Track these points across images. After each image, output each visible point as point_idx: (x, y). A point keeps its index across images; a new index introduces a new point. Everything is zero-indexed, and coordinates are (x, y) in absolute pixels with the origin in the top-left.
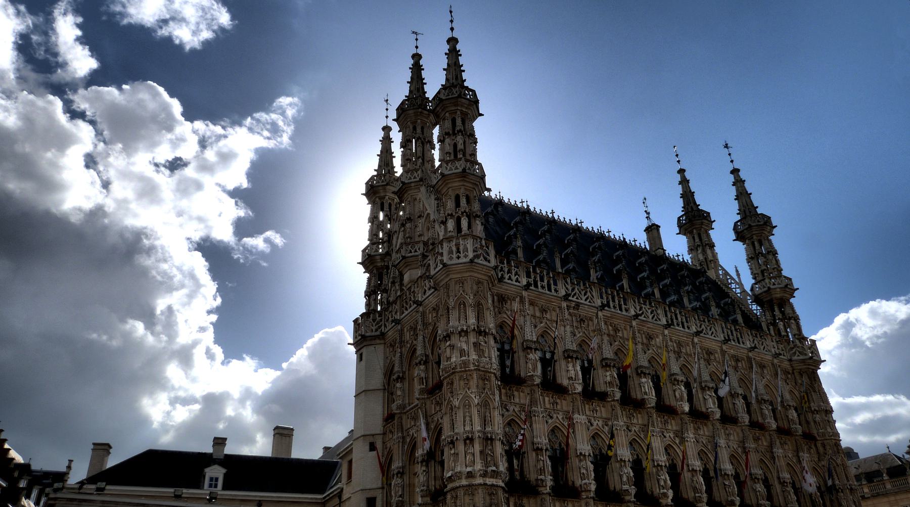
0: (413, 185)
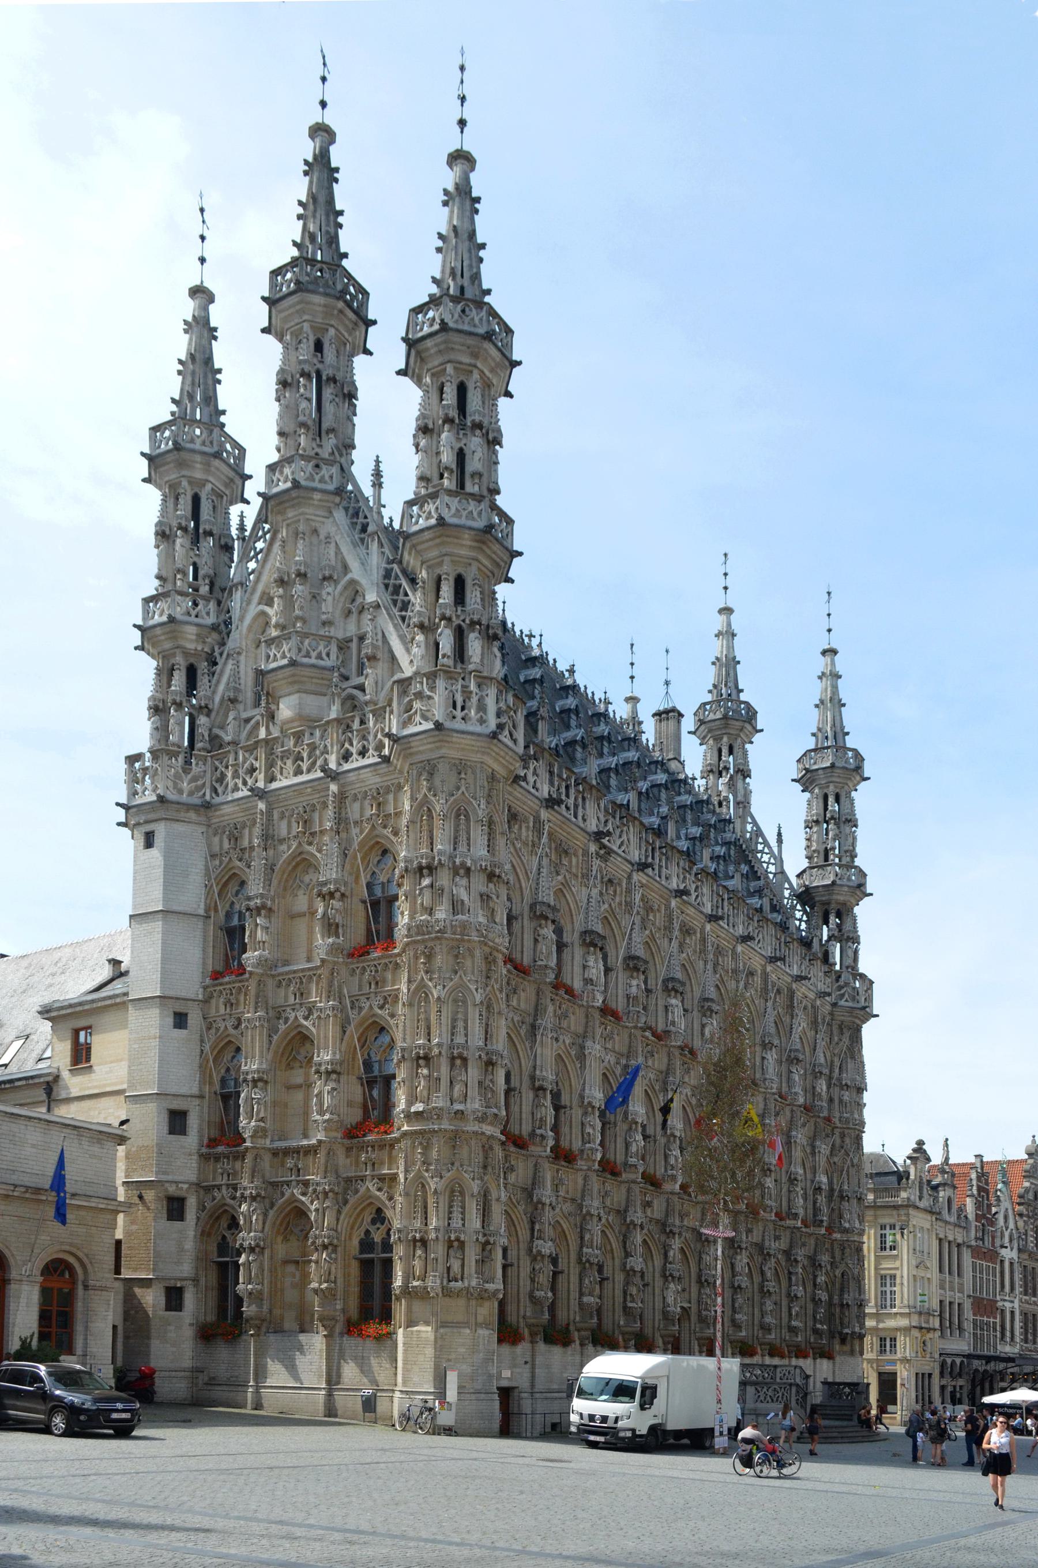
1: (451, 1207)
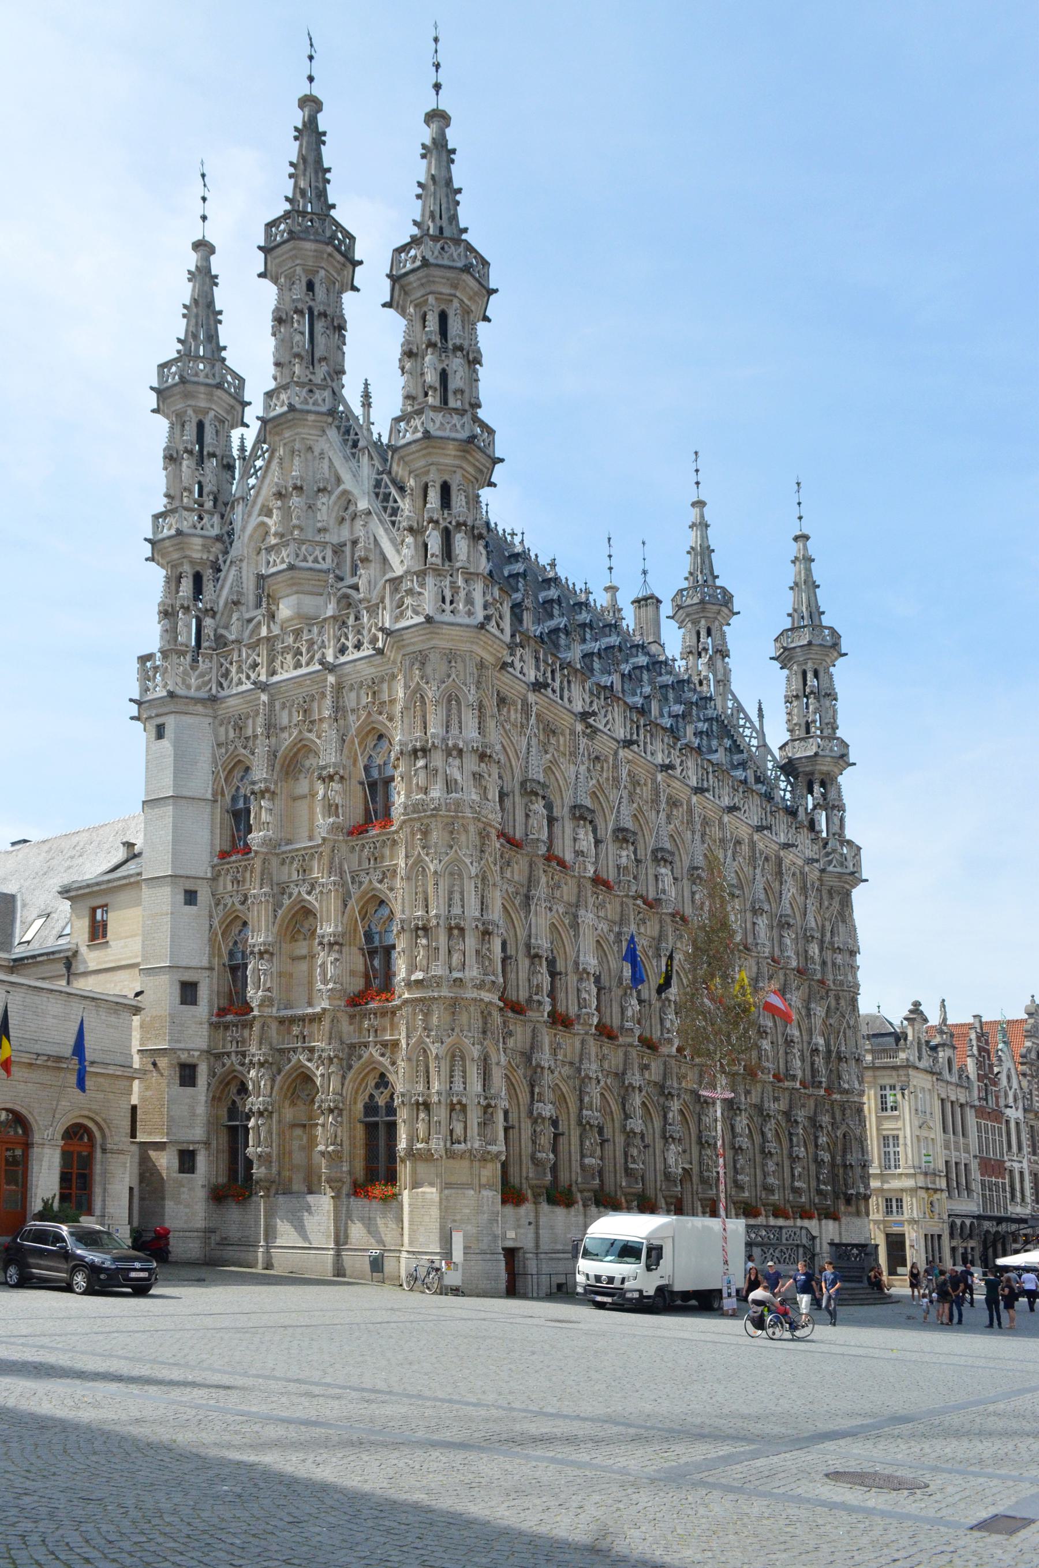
1: (452, 1071)
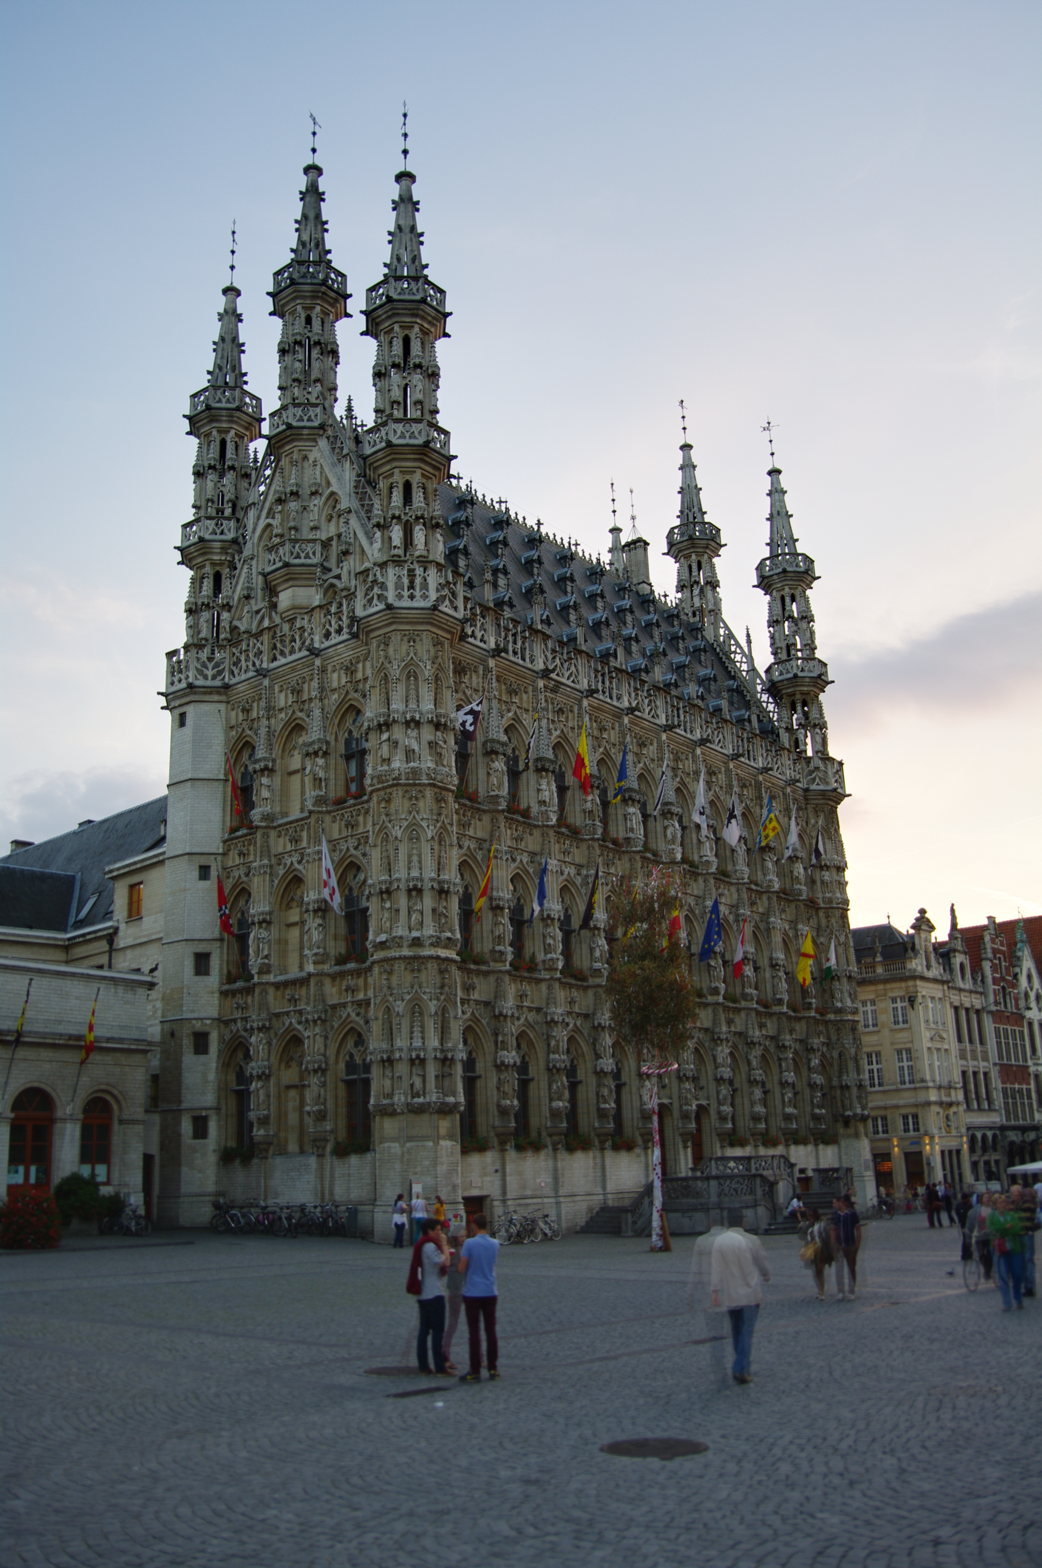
0: (305, 432)
1: (412, 1027)
